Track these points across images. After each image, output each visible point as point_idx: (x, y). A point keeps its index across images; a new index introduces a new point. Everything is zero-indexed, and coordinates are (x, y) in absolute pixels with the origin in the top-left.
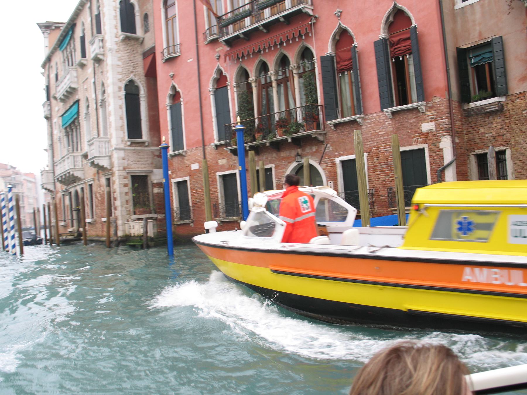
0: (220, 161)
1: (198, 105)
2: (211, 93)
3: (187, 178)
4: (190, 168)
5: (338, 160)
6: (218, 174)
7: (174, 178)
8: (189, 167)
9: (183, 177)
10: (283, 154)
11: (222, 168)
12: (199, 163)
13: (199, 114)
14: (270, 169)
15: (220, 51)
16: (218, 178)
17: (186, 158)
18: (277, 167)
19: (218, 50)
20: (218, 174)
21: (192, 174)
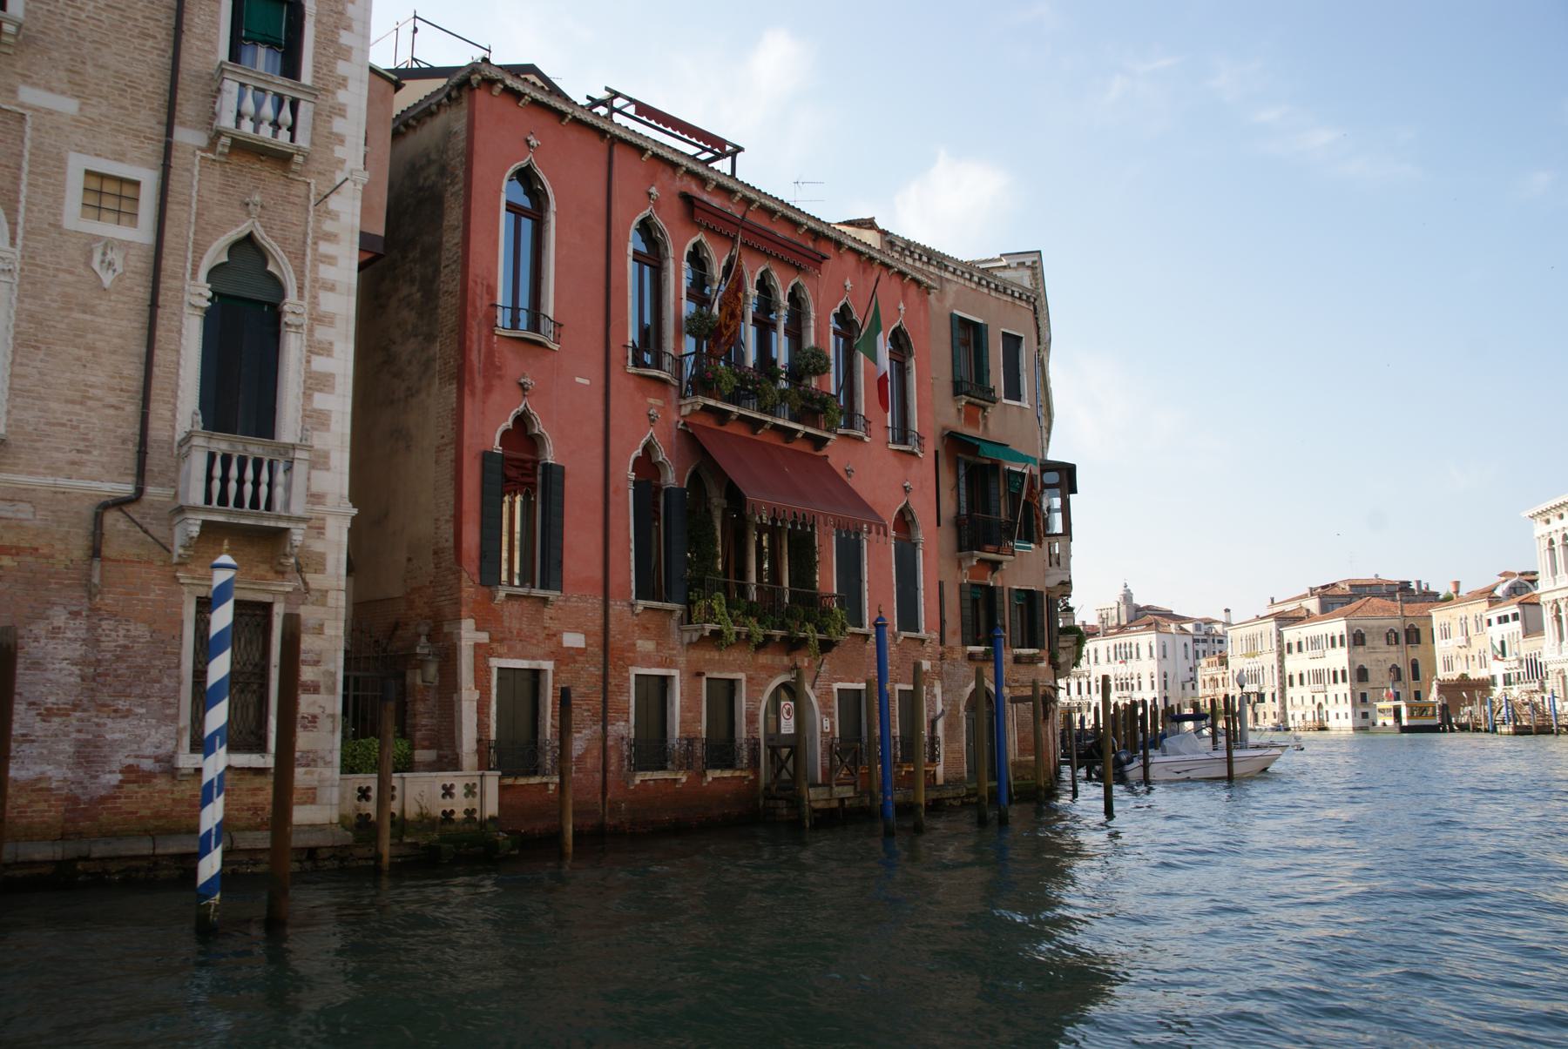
0: (639, 642)
1: (598, 498)
2: (631, 485)
3: (548, 665)
4: (560, 643)
5: (836, 686)
6: (635, 671)
7: (500, 656)
8: (554, 636)
9: (533, 658)
10: (764, 659)
11: (647, 660)
12: (587, 635)
13: (598, 517)
14: (732, 683)
15: (659, 408)
16: (633, 678)
17: (548, 612)
18: (750, 680)
19: (651, 401)
20: (635, 671)
21: (564, 657)
